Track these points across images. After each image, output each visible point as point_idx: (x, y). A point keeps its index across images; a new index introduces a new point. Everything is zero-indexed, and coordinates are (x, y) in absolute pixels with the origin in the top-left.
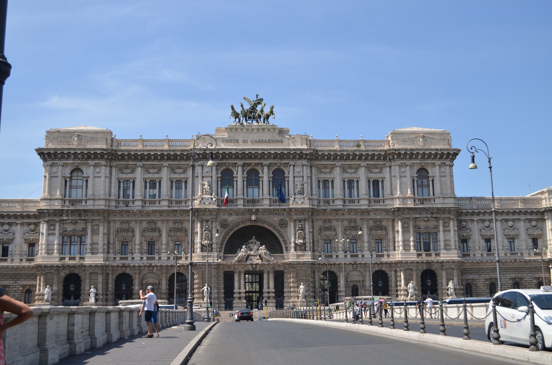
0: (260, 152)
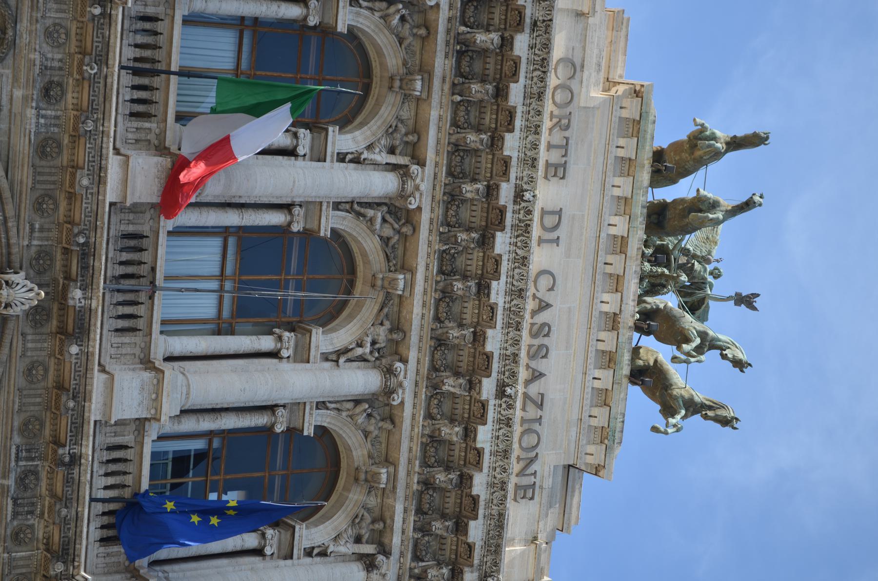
0: (494, 341)
